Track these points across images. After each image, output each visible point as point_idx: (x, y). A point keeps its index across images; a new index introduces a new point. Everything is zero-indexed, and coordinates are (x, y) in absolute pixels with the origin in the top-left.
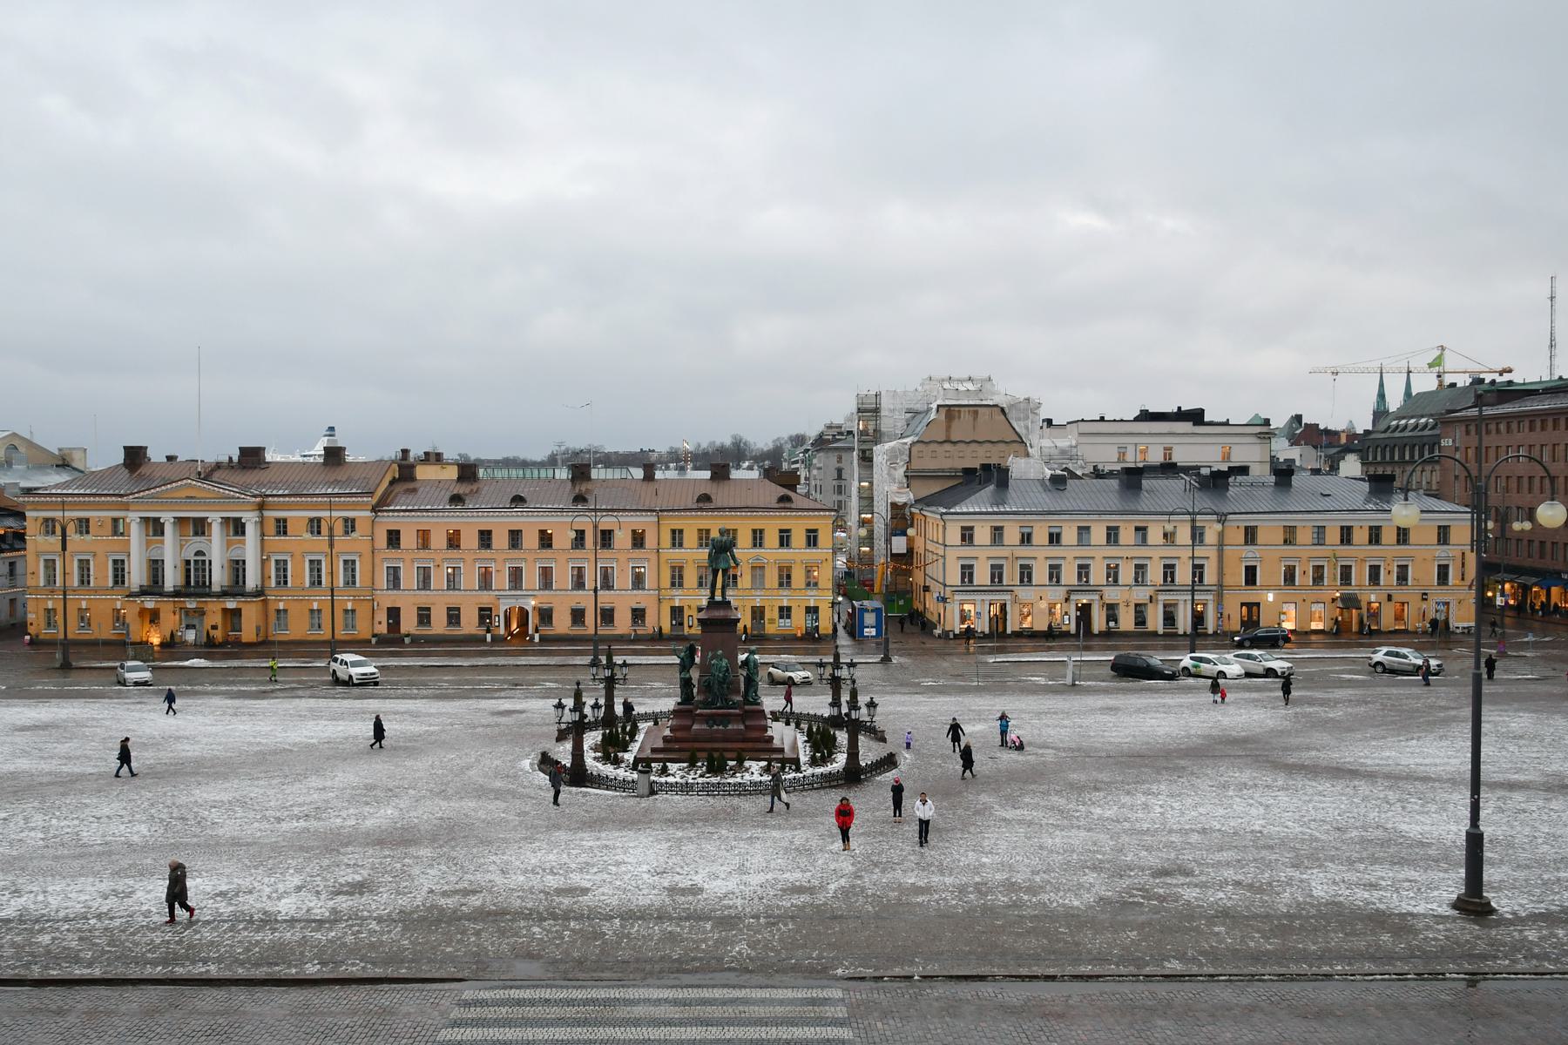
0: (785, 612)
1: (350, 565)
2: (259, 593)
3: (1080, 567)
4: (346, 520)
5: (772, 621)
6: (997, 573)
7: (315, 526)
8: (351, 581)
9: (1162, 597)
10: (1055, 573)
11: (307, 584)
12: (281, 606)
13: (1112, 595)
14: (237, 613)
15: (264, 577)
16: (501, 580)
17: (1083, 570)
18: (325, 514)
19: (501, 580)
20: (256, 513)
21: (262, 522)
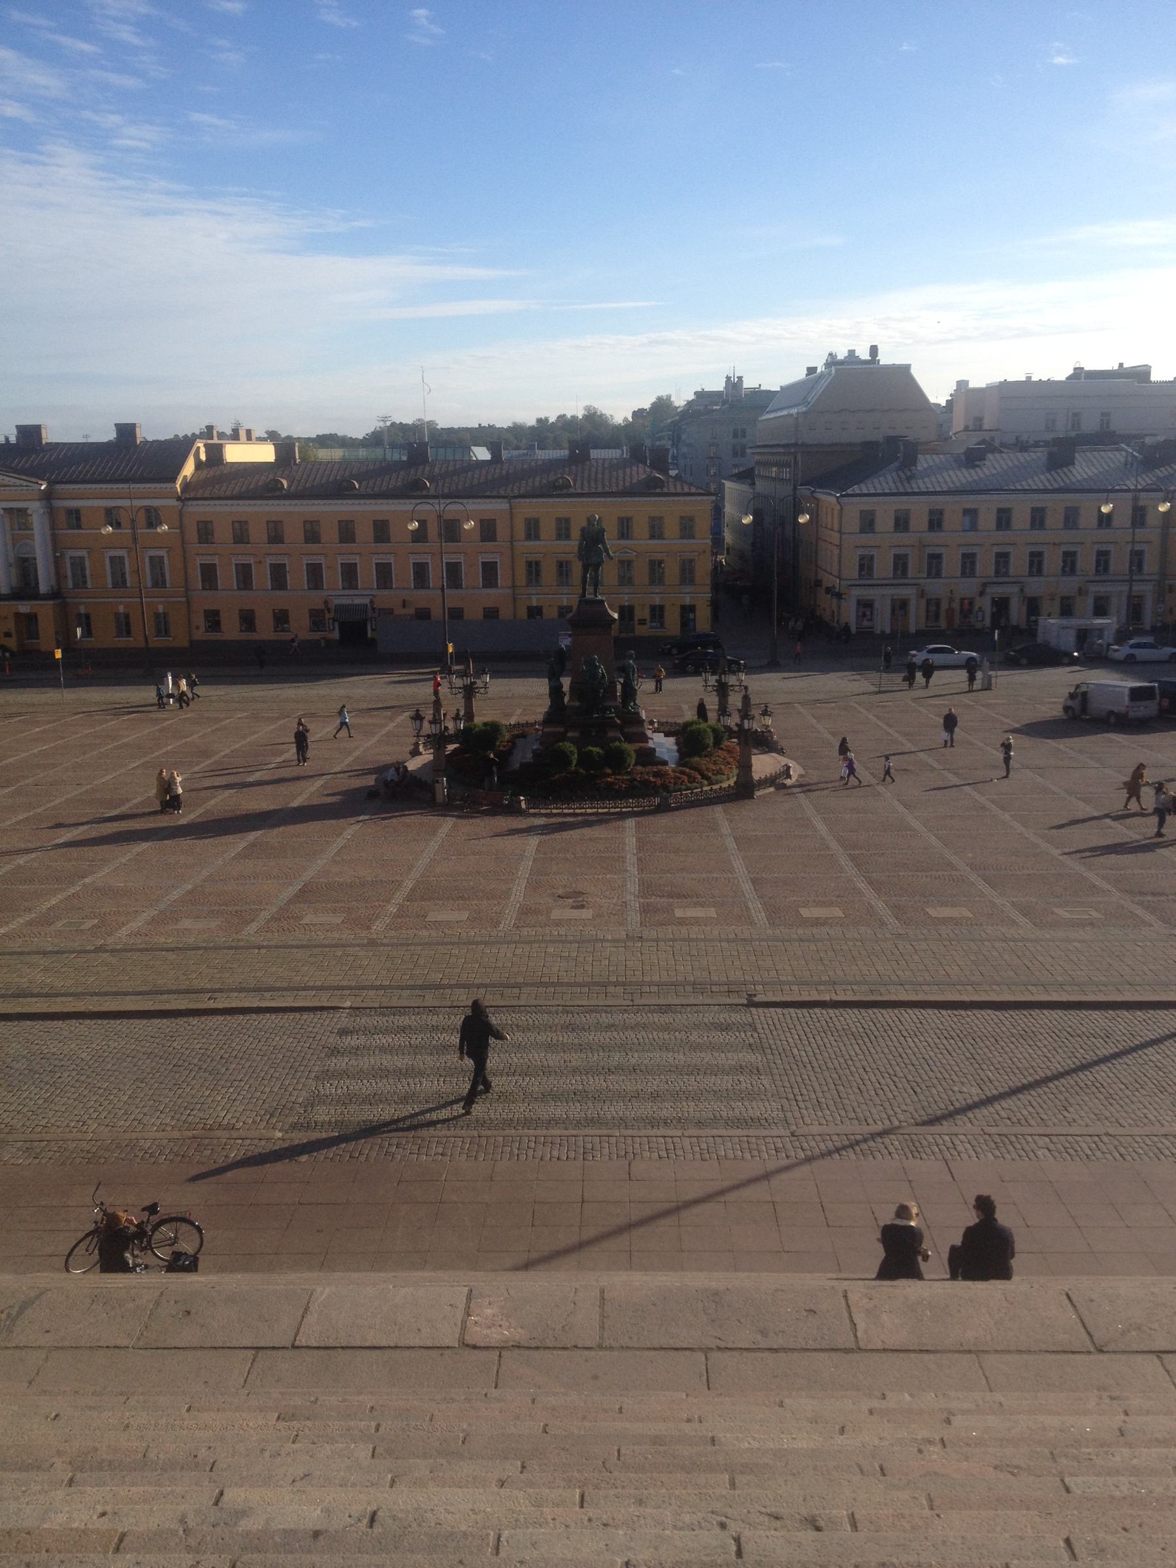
0: (657, 612)
1: (157, 563)
2: (56, 594)
3: (998, 555)
4: (148, 510)
5: (642, 622)
6: (900, 564)
7: (111, 517)
8: (159, 582)
9: (1093, 588)
10: (969, 561)
11: (110, 586)
12: (82, 610)
13: (1036, 587)
14: (32, 618)
15: (59, 576)
16: (332, 577)
17: (1002, 559)
18: (125, 503)
19: (332, 577)
20: (44, 502)
21: (51, 512)
